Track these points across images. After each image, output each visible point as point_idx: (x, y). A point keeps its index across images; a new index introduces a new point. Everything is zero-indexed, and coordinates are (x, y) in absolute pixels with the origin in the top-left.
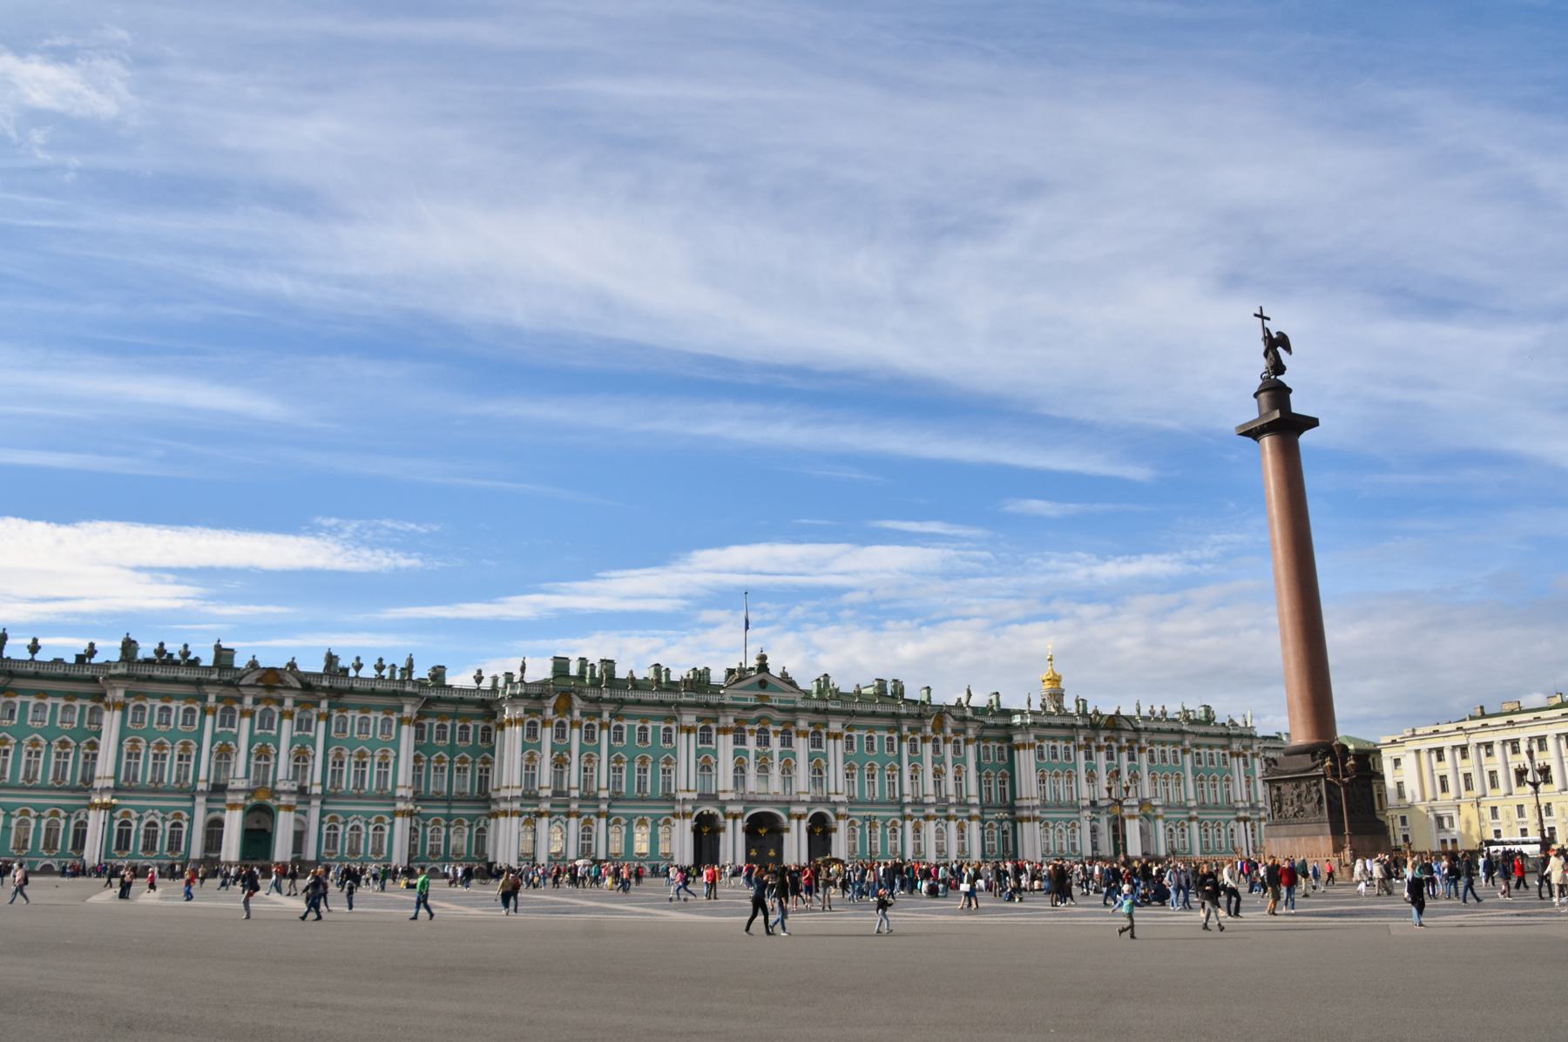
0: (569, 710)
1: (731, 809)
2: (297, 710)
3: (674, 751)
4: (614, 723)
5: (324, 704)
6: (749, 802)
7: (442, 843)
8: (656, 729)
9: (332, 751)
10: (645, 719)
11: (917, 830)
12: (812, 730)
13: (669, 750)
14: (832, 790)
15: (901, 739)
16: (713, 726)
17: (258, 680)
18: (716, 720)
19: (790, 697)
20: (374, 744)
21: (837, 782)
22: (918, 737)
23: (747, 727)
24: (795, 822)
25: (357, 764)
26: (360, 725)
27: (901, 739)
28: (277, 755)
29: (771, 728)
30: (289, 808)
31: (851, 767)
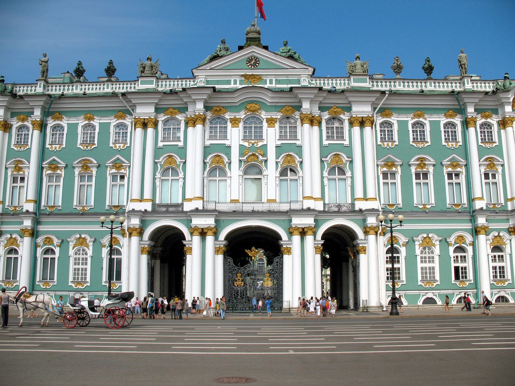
3: (127, 152)
6: (221, 216)
8: (105, 127)
10: (89, 115)
11: (497, 248)
12: (326, 116)
13: (119, 151)
14: (359, 194)
15: (466, 124)
16: (180, 117)
18: (184, 110)
21: (367, 187)
22: (494, 121)
23: (228, 116)
24: (296, 238)
27: (466, 124)
29: (264, 115)
31: (390, 164)
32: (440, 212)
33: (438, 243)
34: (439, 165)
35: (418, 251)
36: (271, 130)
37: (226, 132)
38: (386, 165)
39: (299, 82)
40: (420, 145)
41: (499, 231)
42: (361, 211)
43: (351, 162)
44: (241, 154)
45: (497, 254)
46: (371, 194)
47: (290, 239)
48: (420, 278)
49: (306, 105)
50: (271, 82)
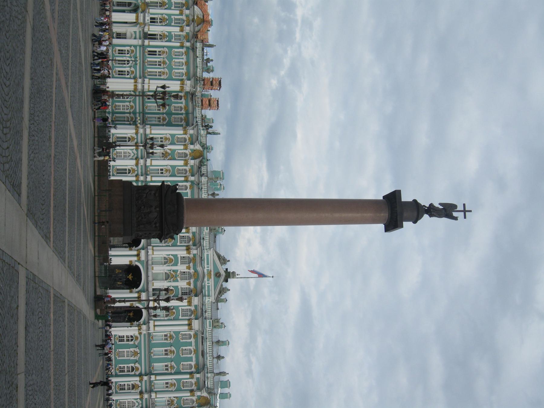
0: (194, 158)
1: (143, 253)
2: (184, 33)
4: (188, 184)
5: (188, 44)
7: (121, 110)
9: (166, 50)
11: (134, 387)
12: (193, 308)
14: (157, 323)
15: (191, 373)
16: (191, 243)
17: (198, 17)
18: (194, 245)
19: (212, 292)
20: (170, 68)
22: (194, 387)
23: (191, 264)
25: (159, 62)
26: (179, 62)
27: (191, 373)
28: (162, 25)
30: (137, 18)
31: (171, 337)
32: (150, 361)
33: (135, 358)
34: (171, 360)
35: (132, 349)
36: (185, 283)
37: (184, 264)
38: (170, 336)
39: (209, 296)
40: (180, 352)
41: (141, 387)
42: (149, 323)
43: (171, 320)
44: (173, 271)
45: (131, 387)
46: (157, 328)
47: (136, 292)
48: (120, 350)
49: (196, 298)
50: (208, 283)
